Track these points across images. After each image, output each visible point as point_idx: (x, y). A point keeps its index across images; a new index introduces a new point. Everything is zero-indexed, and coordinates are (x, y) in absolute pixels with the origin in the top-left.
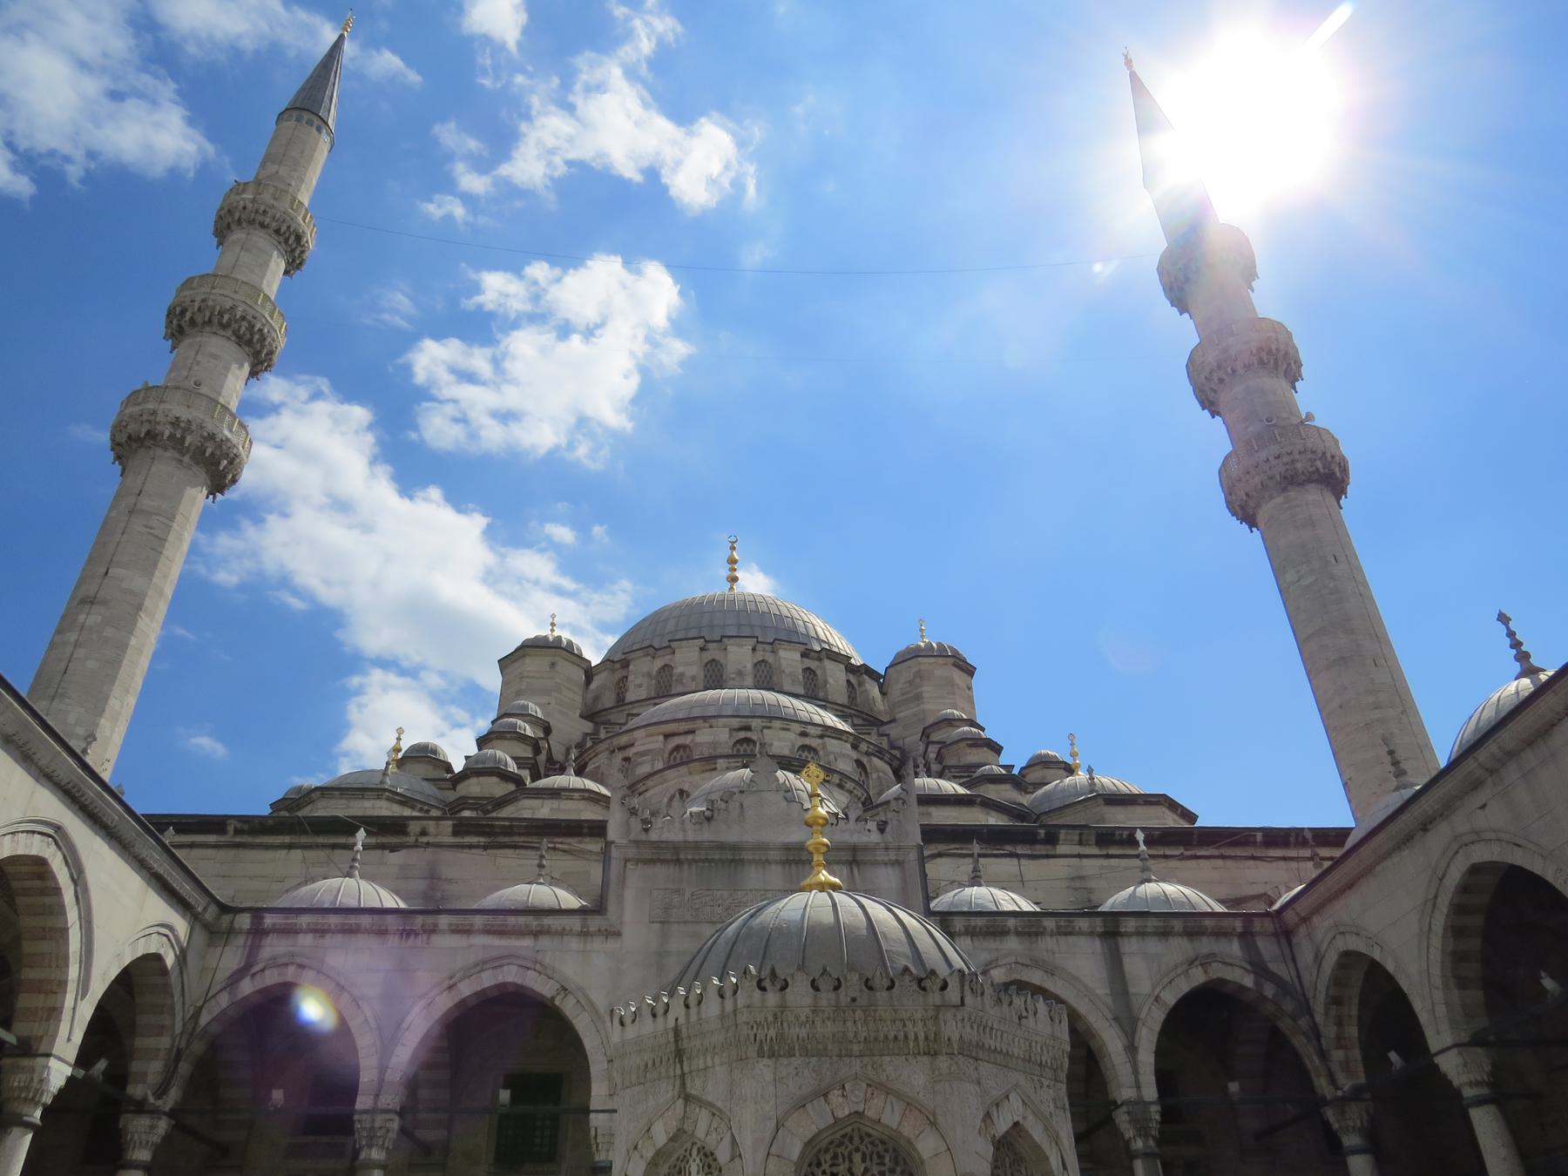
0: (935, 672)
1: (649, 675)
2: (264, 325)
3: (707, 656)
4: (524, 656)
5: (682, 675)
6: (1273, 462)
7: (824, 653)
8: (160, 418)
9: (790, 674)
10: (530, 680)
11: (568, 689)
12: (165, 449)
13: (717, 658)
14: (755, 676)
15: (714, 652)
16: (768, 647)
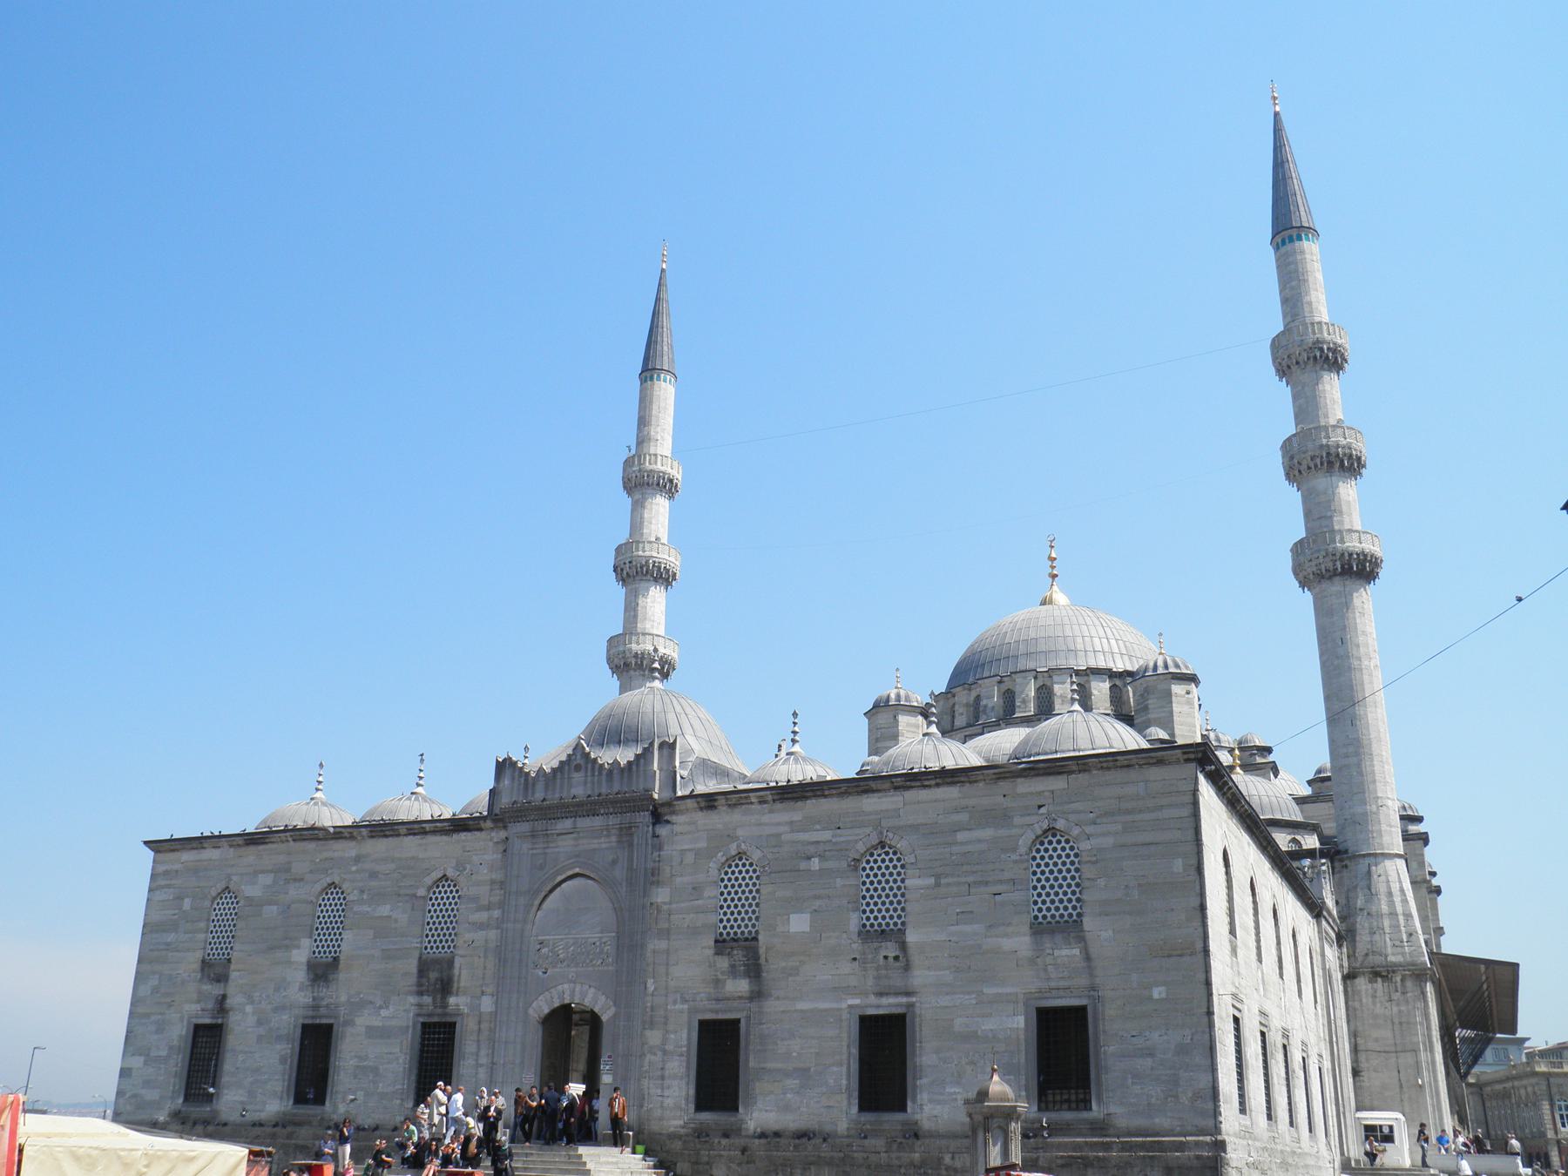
0: (1158, 686)
1: (967, 705)
2: (666, 564)
3: (1004, 687)
4: (877, 713)
5: (986, 706)
6: (1307, 564)
7: (1088, 671)
8: (628, 655)
9: (1061, 696)
10: (883, 730)
11: (908, 731)
12: (635, 670)
13: (1010, 687)
14: (1039, 698)
15: (1007, 684)
16: (1046, 674)
